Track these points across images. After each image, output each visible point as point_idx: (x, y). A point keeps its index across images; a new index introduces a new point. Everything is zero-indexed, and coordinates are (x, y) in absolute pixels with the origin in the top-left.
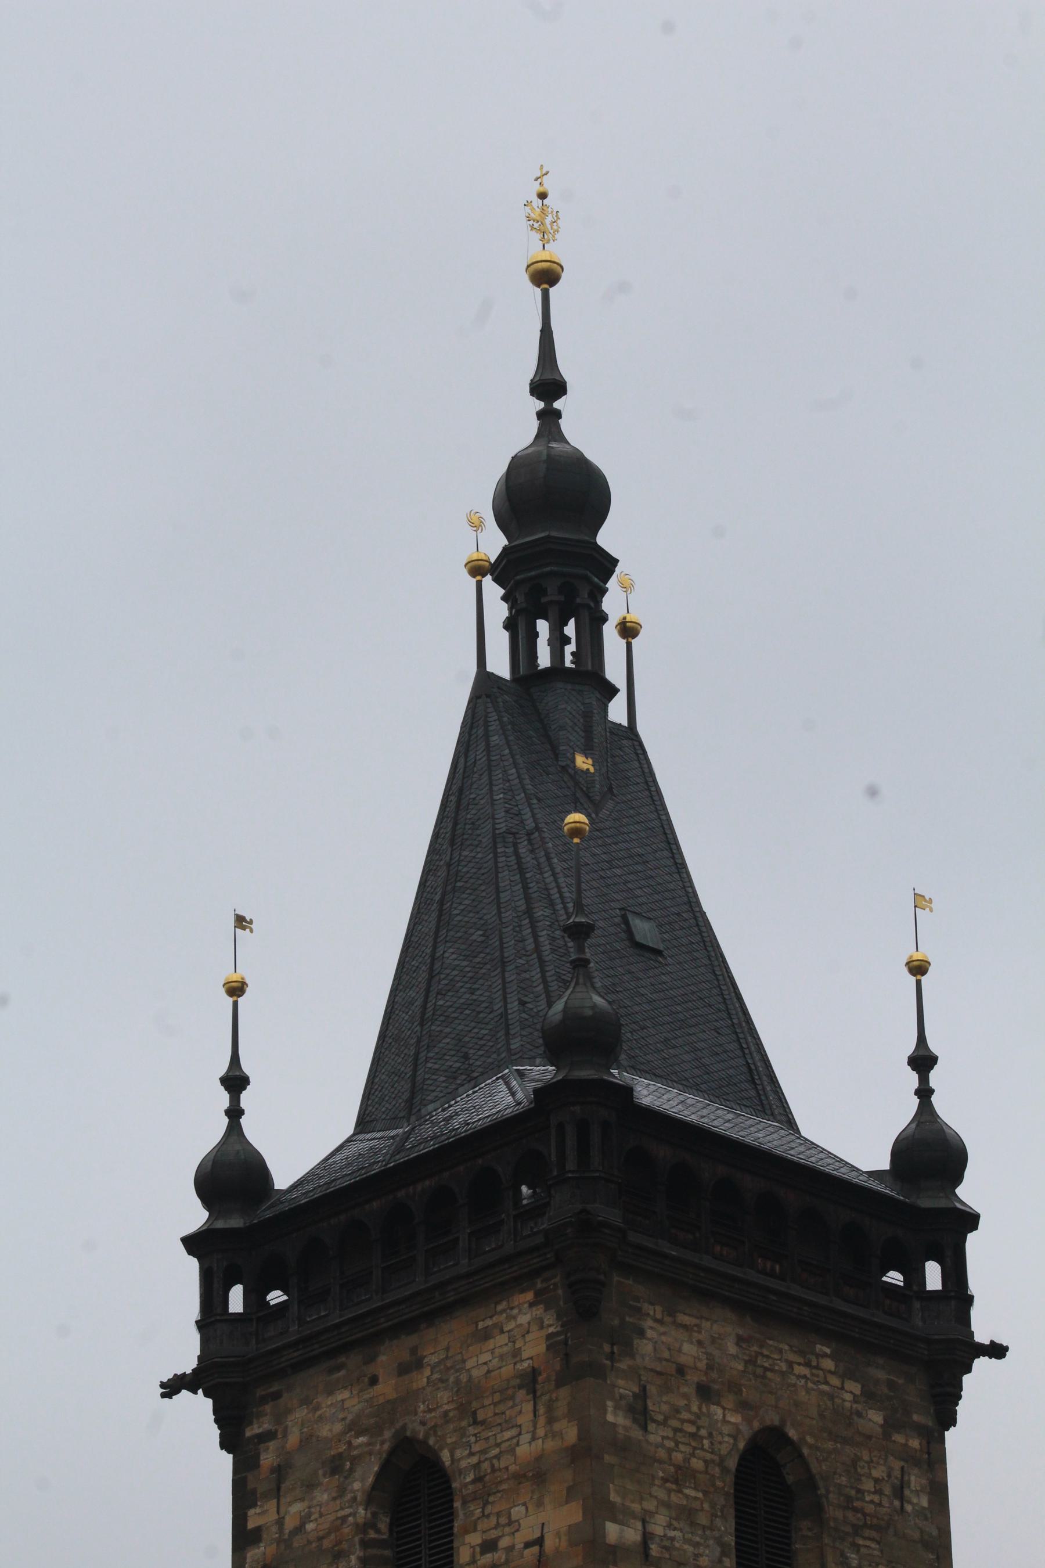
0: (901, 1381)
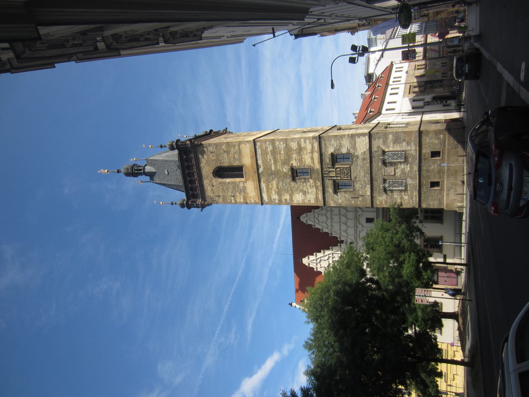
0: (199, 152)
